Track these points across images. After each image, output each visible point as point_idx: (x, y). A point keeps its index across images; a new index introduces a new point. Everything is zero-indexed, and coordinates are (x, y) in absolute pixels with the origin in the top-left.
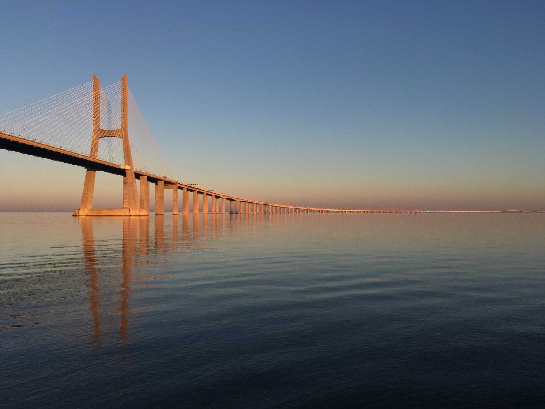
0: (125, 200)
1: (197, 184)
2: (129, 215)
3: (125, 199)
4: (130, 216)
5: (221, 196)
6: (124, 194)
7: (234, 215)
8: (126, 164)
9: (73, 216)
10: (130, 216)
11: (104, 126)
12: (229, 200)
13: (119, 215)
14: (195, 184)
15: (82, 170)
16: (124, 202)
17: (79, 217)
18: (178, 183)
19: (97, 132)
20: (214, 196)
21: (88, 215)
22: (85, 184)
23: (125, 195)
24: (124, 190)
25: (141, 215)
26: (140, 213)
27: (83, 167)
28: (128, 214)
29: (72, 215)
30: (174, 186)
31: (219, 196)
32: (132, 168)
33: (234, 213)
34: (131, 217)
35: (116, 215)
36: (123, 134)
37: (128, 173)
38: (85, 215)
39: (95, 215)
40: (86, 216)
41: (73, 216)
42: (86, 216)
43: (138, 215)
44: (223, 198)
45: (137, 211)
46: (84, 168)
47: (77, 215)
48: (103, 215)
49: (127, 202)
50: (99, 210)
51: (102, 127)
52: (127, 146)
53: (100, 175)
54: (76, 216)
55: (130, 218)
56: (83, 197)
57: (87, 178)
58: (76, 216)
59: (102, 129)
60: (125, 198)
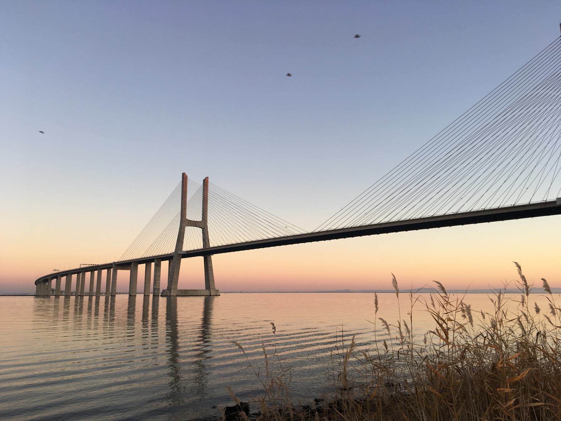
0: (157, 281)
2: (210, 295)
3: (157, 280)
4: (211, 295)
10: (211, 295)
13: (202, 295)
17: (171, 297)
23: (157, 277)
25: (218, 295)
26: (217, 293)
38: (176, 295)
39: (183, 295)
47: (169, 295)
48: (189, 295)
49: (157, 283)
54: (168, 296)
55: (210, 297)
58: (168, 296)
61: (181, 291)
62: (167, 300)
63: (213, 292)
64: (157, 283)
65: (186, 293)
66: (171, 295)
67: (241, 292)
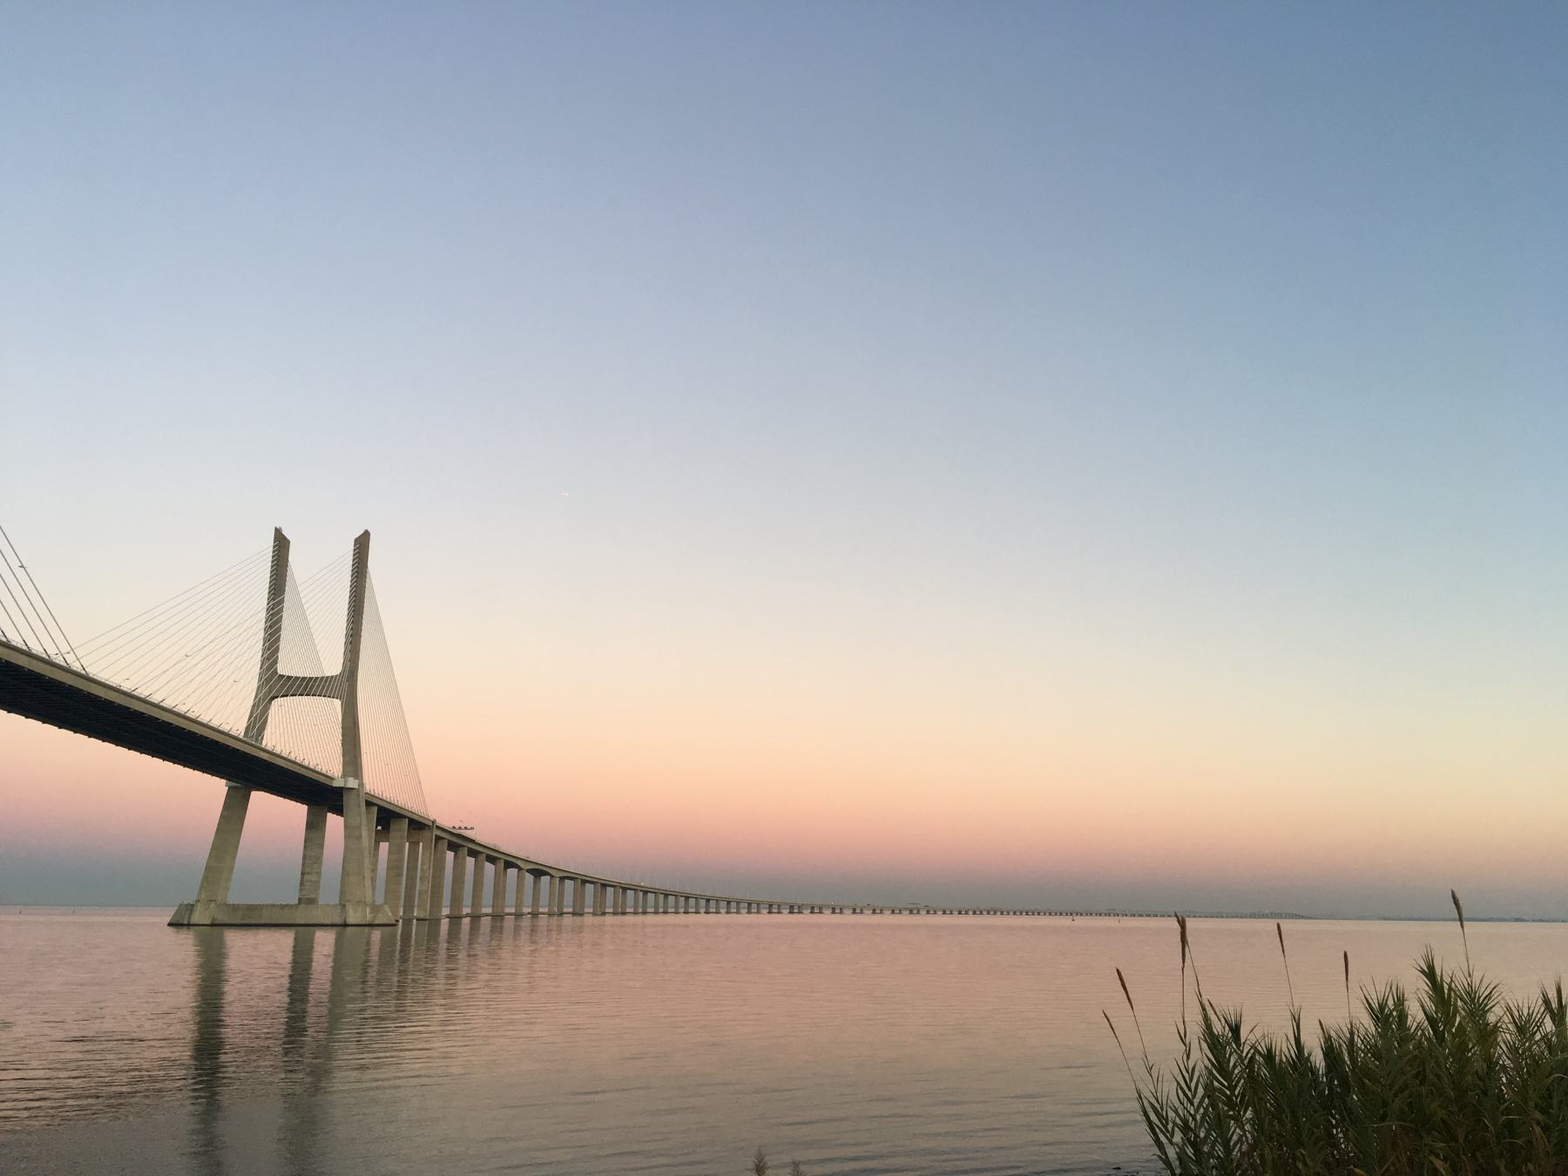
1: (469, 827)
3: (308, 873)
4: (345, 925)
5: (519, 863)
6: (304, 857)
7: (543, 921)
8: (344, 775)
9: (169, 925)
10: (345, 925)
11: (288, 666)
12: (532, 874)
14: (466, 828)
15: (212, 789)
16: (302, 884)
18: (437, 826)
19: (268, 680)
20: (502, 862)
21: (218, 923)
22: (218, 830)
24: (305, 847)
25: (376, 922)
26: (375, 917)
27: (221, 778)
28: (338, 920)
29: (168, 920)
30: (426, 833)
31: (514, 861)
32: (361, 785)
33: (543, 914)
34: (349, 929)
35: (302, 922)
36: (344, 687)
37: (349, 802)
39: (238, 921)
40: (212, 925)
41: (169, 925)
42: (212, 925)
43: (367, 923)
44: (520, 869)
45: (368, 910)
46: (224, 781)
47: (186, 922)
48: (263, 922)
49: (310, 881)
50: (252, 908)
51: (285, 667)
52: (355, 724)
53: (262, 803)
56: (208, 868)
57: (226, 813)
59: (280, 672)
60: (307, 870)
61: (235, 908)
62: (296, 934)
63: (355, 912)
64: (308, 884)
65: (252, 920)
66: (192, 922)
67: (1517, 920)
